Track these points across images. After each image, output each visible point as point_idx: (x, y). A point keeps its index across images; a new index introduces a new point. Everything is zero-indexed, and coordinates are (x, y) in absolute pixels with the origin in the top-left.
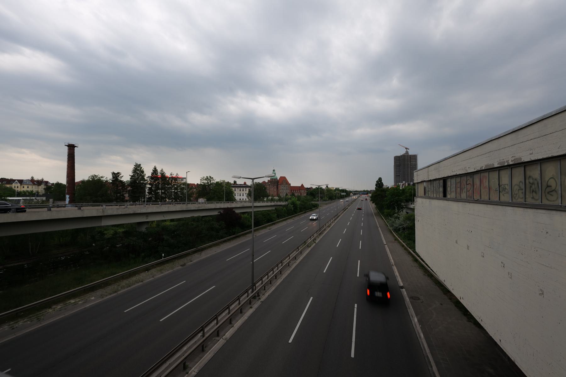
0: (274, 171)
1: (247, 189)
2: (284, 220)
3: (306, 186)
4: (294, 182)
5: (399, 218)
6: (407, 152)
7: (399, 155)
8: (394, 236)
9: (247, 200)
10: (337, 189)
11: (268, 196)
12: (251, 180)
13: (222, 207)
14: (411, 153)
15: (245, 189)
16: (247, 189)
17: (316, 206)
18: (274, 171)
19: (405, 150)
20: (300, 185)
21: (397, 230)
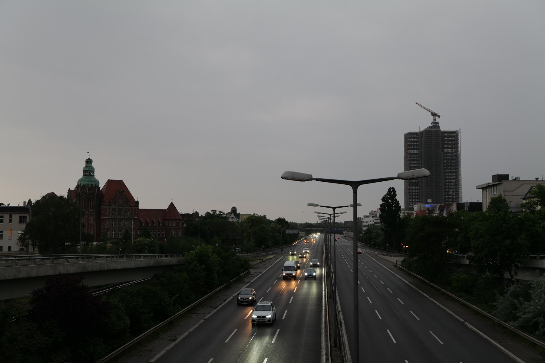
0: (89, 162)
1: (16, 217)
2: (190, 312)
3: (183, 209)
4: (149, 197)
5: (528, 298)
6: (435, 125)
7: (416, 130)
8: (534, 345)
9: (15, 248)
10: (281, 221)
11: (88, 239)
12: (349, 188)
13: (34, 274)
14: (444, 127)
15: (6, 217)
16: (16, 217)
17: (245, 266)
18: (89, 162)
19: (431, 119)
20: (165, 207)
21: (531, 327)
